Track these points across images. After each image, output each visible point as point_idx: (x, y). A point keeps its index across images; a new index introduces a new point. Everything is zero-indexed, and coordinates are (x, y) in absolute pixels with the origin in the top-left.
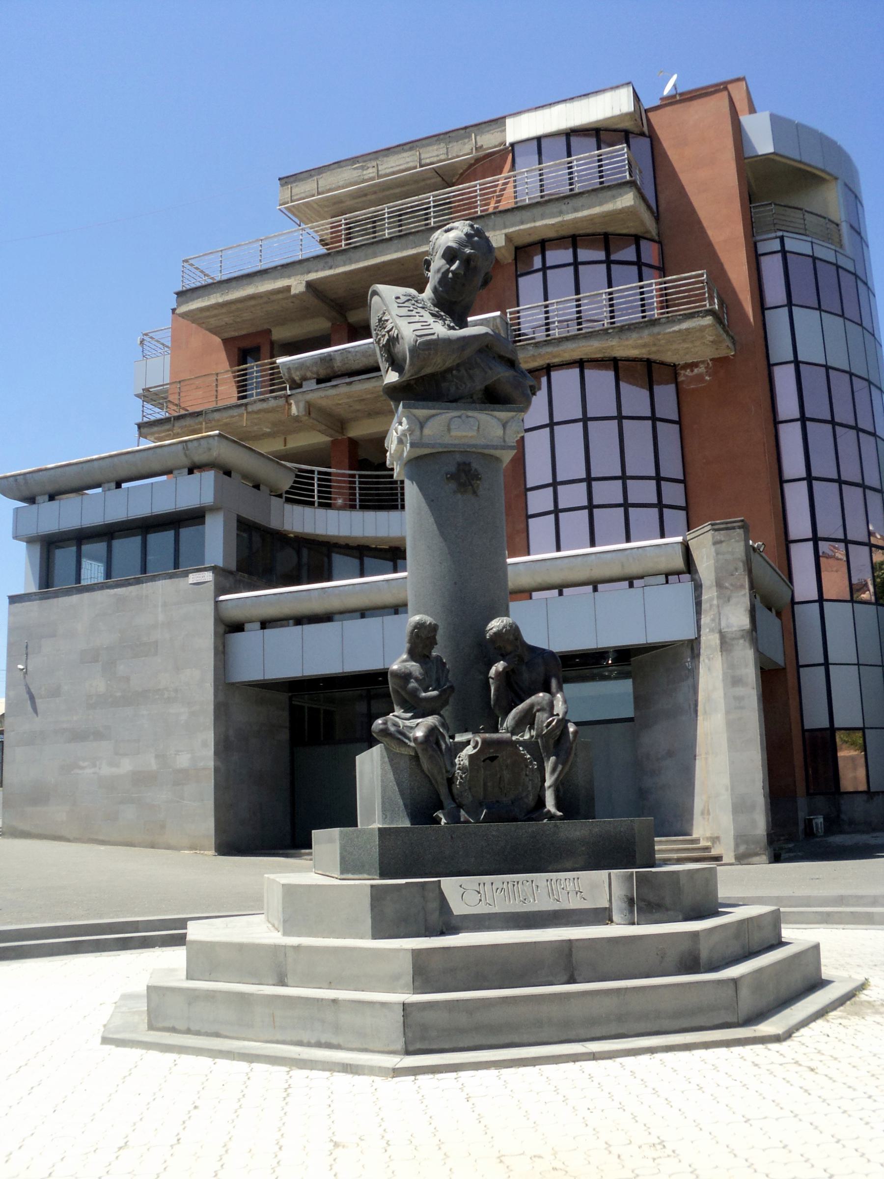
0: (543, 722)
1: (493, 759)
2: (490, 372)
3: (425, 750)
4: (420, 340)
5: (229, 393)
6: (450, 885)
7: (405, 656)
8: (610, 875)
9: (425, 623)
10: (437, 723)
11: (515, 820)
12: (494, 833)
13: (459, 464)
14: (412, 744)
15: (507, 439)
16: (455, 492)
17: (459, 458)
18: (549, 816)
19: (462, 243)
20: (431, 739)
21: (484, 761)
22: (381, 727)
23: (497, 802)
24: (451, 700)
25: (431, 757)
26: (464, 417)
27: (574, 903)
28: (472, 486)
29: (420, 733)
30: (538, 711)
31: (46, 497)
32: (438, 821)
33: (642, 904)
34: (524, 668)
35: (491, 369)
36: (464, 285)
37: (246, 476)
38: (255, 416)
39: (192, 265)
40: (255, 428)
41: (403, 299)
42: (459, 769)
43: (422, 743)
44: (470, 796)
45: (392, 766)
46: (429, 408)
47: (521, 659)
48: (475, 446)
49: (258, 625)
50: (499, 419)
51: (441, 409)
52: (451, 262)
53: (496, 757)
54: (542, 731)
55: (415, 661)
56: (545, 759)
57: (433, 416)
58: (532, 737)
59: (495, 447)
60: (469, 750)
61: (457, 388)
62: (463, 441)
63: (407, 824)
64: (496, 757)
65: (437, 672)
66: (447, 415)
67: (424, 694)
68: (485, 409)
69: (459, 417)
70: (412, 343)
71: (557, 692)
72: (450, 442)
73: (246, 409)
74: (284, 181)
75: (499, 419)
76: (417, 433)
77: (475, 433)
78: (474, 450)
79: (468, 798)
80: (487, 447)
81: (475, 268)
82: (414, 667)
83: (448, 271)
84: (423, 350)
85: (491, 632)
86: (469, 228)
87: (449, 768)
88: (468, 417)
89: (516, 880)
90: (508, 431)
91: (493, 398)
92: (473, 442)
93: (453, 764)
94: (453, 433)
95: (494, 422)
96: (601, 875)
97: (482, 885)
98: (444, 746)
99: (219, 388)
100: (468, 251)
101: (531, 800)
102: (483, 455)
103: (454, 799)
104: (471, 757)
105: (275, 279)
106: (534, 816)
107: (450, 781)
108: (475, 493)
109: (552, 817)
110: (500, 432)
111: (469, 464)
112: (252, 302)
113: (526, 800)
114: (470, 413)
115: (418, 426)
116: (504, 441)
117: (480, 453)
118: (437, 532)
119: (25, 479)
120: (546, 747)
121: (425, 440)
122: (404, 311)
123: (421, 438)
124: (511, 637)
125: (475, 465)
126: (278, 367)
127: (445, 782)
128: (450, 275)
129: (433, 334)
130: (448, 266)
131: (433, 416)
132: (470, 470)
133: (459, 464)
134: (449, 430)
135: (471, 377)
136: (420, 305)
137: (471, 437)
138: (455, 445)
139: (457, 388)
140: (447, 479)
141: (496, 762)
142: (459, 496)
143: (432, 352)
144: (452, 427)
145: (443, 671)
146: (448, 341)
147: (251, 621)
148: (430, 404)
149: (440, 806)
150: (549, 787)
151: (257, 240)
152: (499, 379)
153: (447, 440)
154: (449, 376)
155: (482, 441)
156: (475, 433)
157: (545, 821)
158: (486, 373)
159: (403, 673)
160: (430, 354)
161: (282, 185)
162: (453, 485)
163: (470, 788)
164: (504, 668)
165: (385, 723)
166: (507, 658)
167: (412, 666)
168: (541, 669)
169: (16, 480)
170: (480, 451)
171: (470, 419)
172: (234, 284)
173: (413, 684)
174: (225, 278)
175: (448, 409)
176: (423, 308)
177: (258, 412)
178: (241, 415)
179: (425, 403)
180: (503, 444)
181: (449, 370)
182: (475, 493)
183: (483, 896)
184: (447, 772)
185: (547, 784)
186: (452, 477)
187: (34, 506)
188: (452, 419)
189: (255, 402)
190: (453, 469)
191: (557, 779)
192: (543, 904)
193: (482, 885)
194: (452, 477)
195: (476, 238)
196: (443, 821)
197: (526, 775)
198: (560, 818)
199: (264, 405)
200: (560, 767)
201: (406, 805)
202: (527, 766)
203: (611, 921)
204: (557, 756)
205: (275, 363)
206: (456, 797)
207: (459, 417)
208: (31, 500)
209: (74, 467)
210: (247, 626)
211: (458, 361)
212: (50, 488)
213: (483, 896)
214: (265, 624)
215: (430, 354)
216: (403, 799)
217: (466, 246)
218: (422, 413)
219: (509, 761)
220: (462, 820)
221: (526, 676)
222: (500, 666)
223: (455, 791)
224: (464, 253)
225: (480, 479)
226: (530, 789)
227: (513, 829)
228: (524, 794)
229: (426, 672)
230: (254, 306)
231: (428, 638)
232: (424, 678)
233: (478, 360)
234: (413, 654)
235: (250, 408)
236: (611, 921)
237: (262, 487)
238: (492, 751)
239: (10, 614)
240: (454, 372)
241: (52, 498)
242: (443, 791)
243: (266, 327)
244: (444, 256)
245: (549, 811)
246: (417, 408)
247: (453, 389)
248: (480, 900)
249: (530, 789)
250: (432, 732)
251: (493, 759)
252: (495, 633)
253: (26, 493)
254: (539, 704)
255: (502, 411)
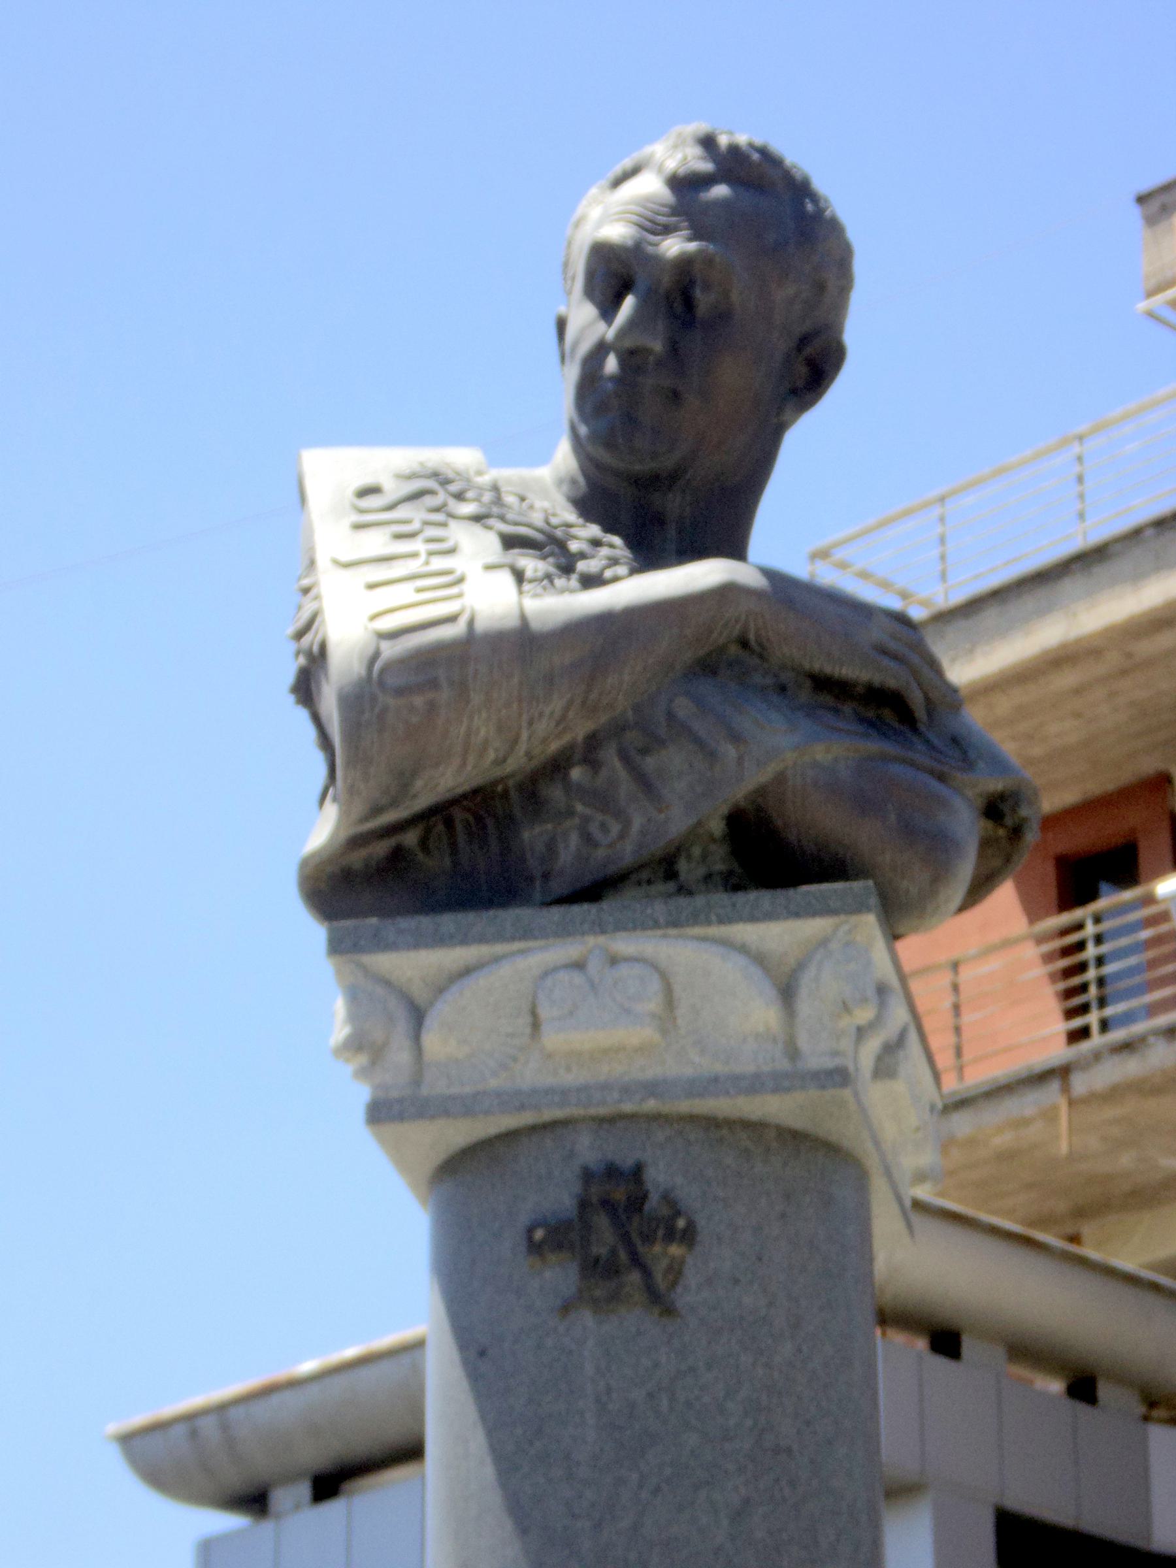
2: (730, 751)
4: (390, 650)
5: (1042, 1033)
13: (587, 1176)
15: (803, 1042)
16: (566, 1309)
17: (588, 1150)
19: (655, 225)
26: (594, 966)
28: (647, 1273)
31: (304, 1490)
35: (736, 738)
36: (675, 396)
37: (1027, 1351)
38: (1111, 1112)
39: (843, 565)
40: (1126, 1160)
41: (393, 490)
46: (440, 940)
48: (652, 1088)
50: (760, 959)
51: (500, 937)
52: (608, 311)
57: (467, 972)
59: (754, 1084)
61: (588, 839)
62: (607, 1071)
66: (522, 963)
68: (695, 919)
69: (579, 965)
70: (358, 669)
72: (548, 1080)
73: (1066, 1089)
74: (1155, 205)
75: (760, 959)
76: (400, 1055)
77: (646, 1033)
78: (651, 1105)
80: (713, 1085)
81: (723, 316)
83: (601, 349)
84: (400, 692)
86: (697, 151)
88: (614, 960)
90: (805, 1006)
91: (767, 856)
92: (653, 1072)
94: (553, 1039)
95: (729, 970)
99: (967, 1018)
100: (674, 246)
102: (711, 1123)
105: (1137, 577)
108: (660, 1301)
110: (763, 1013)
111: (637, 1172)
112: (1067, 679)
114: (625, 944)
115: (402, 1027)
116: (793, 1052)
117: (693, 1119)
118: (495, 1499)
119: (225, 1427)
121: (436, 1086)
122: (377, 542)
123: (417, 1081)
125: (658, 1177)
126: (1164, 917)
128: (611, 364)
129: (452, 619)
130: (601, 326)
131: (467, 972)
132: (637, 1202)
133: (587, 1176)
134: (536, 1025)
135: (645, 784)
136: (468, 509)
137: (641, 1050)
138: (563, 1094)
139: (588, 839)
140: (535, 1248)
142: (586, 1318)
143: (445, 695)
144: (544, 1012)
146: (521, 643)
148: (448, 921)
151: (1064, 442)
152: (780, 779)
153: (531, 1074)
154: (555, 793)
155: (699, 1064)
156: (646, 1033)
158: (712, 756)
160: (432, 707)
161: (1151, 221)
162: (560, 1275)
169: (194, 1434)
170: (685, 1106)
171: (624, 970)
172: (990, 616)
174: (958, 597)
175: (526, 934)
176: (477, 518)
177: (1114, 1094)
178: (1050, 1115)
179: (425, 922)
180: (784, 1065)
181: (557, 767)
182: (660, 1301)
186: (551, 1239)
187: (267, 1527)
188: (546, 974)
189: (1097, 1056)
190: (560, 1197)
194: (551, 1239)
195: (720, 191)
199: (1130, 1067)
205: (1150, 900)
207: (579, 965)
208: (254, 1501)
209: (385, 1366)
211: (581, 730)
212: (319, 1454)
215: (432, 707)
217: (667, 230)
218: (412, 964)
224: (657, 259)
225: (689, 1236)
230: (1078, 691)
233: (683, 707)
235: (1080, 1084)
237: (1104, 1391)
240: (576, 773)
241: (327, 1485)
243: (1148, 765)
244: (590, 292)
246: (392, 947)
247: (569, 850)
253: (235, 1479)
255: (769, 916)
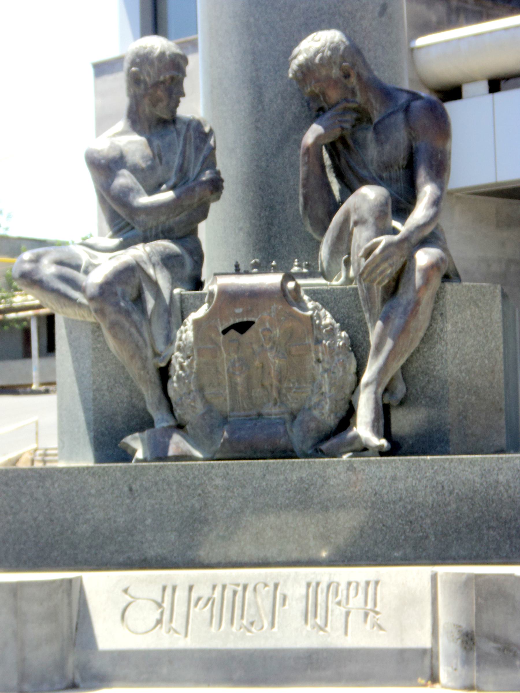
0: (359, 247)
1: (242, 327)
3: (101, 312)
6: (100, 587)
7: (122, 124)
8: (434, 578)
9: (150, 53)
10: (145, 258)
11: (287, 453)
12: (218, 481)
14: (84, 301)
18: (357, 446)
20: (119, 289)
21: (225, 332)
22: (27, 267)
23: (260, 415)
24: (214, 208)
25: (113, 326)
27: (360, 637)
29: (95, 279)
30: (356, 223)
32: (126, 456)
33: (489, 647)
34: (370, 135)
42: (179, 349)
43: (91, 299)
44: (200, 407)
45: (70, 344)
47: (362, 117)
49: (484, 86)
53: (250, 324)
54: (359, 265)
55: (140, 133)
56: (369, 325)
58: (349, 280)
60: (203, 311)
63: (86, 459)
64: (250, 324)
65: (183, 153)
67: (144, 200)
71: (425, 183)
79: (191, 410)
82: (134, 145)
85: (294, 65)
87: (160, 347)
89: (242, 581)
93: (169, 340)
96: (415, 578)
97: (169, 591)
98: (150, 303)
101: (327, 415)
103: (171, 410)
104: (197, 323)
106: (324, 447)
107: (164, 374)
109: (363, 450)
113: (316, 413)
120: (369, 299)
124: (335, 72)
127: (155, 377)
141: (250, 333)
145: (198, 150)
147: (473, 80)
149: (144, 423)
150: (367, 385)
157: (345, 457)
159: (104, 158)
163: (201, 390)
164: (318, 138)
165: (37, 260)
166: (328, 115)
167: (130, 143)
168: (400, 136)
173: (124, 179)
183: (166, 617)
184: (156, 355)
185: (366, 378)
191: (383, 371)
192: (292, 634)
193: (169, 591)
196: (139, 455)
197: (318, 361)
198: (382, 453)
200: (389, 344)
201: (88, 424)
202: (318, 342)
203: (434, 679)
204: (386, 320)
206: (174, 406)
210: (466, 90)
213: (166, 617)
214: (495, 85)
216: (86, 410)
219: (277, 332)
220: (171, 452)
221: (372, 152)
222: (314, 132)
223: (171, 393)
226: (326, 388)
227: (258, 474)
228: (315, 399)
229: (158, 156)
231: (156, 85)
232: (152, 168)
234: (136, 120)
236: (434, 679)
238: (239, 310)
239: (99, 94)
242: (150, 395)
245: (357, 437)
248: (159, 622)
249: (326, 388)
250: (129, 273)
251: (242, 327)
252: (300, 66)
254: (356, 210)
